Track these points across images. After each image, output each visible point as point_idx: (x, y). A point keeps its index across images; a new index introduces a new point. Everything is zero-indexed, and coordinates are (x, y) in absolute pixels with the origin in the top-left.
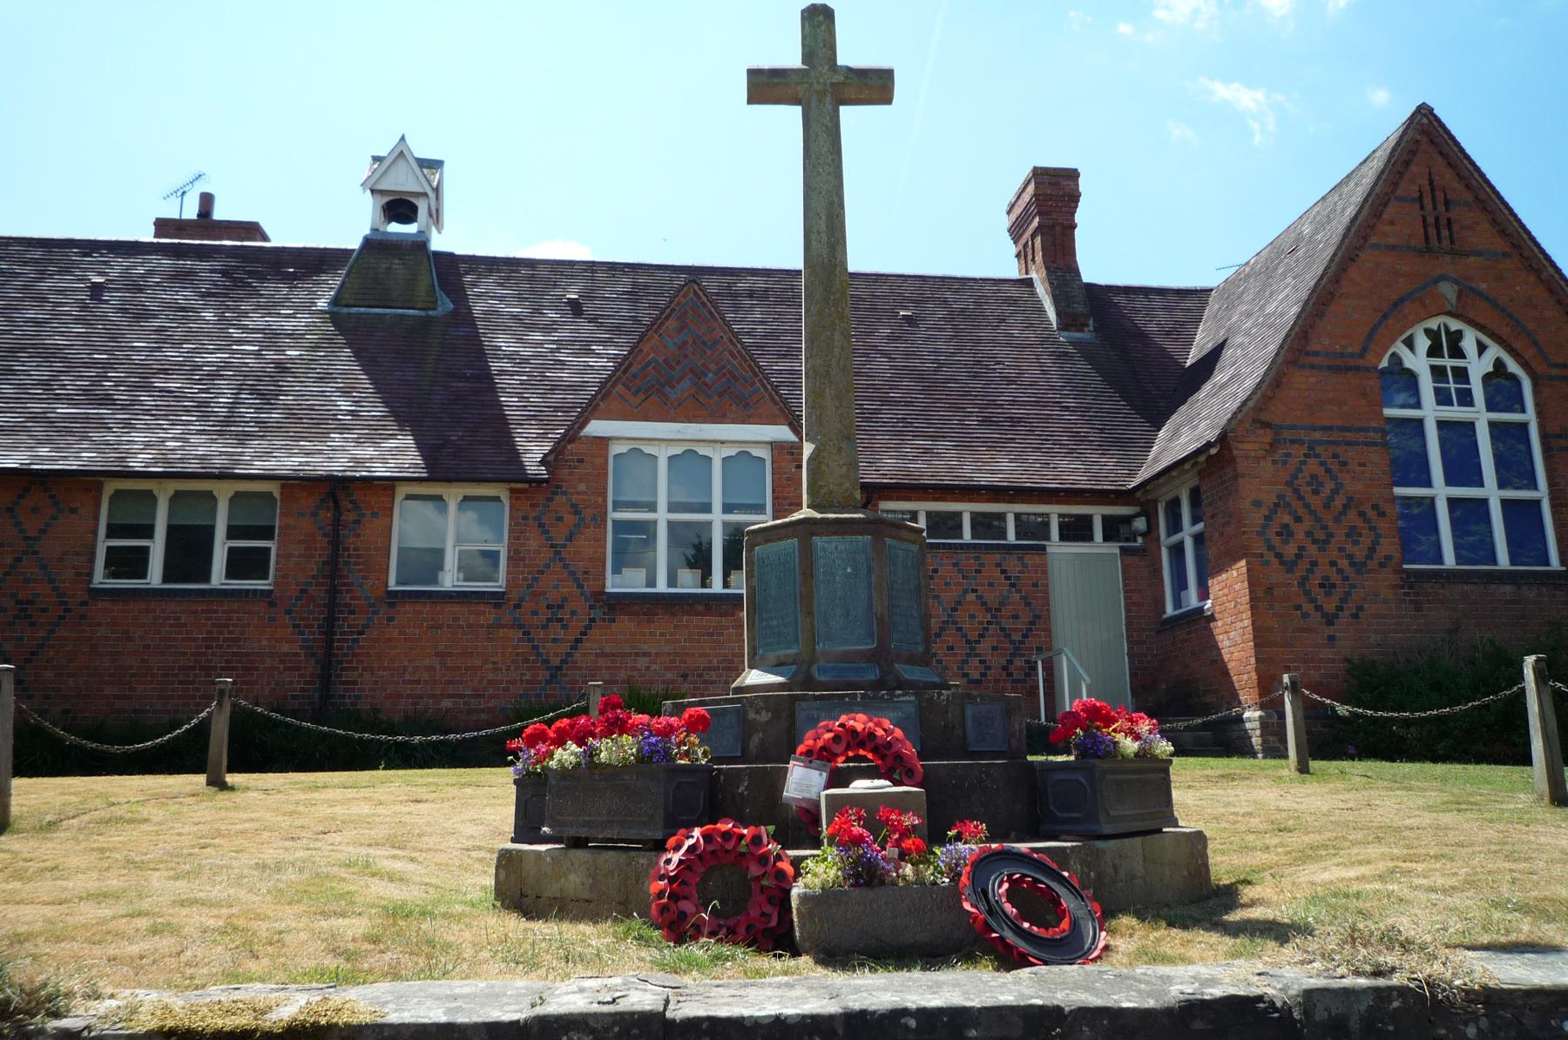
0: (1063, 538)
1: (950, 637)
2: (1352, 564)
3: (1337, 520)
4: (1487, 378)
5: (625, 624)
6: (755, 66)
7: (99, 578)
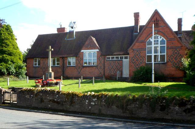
0: (125, 59)
1: (112, 69)
2: (140, 63)
3: (139, 58)
4: (161, 41)
5: (85, 68)
6: (140, 14)
7: (34, 66)
